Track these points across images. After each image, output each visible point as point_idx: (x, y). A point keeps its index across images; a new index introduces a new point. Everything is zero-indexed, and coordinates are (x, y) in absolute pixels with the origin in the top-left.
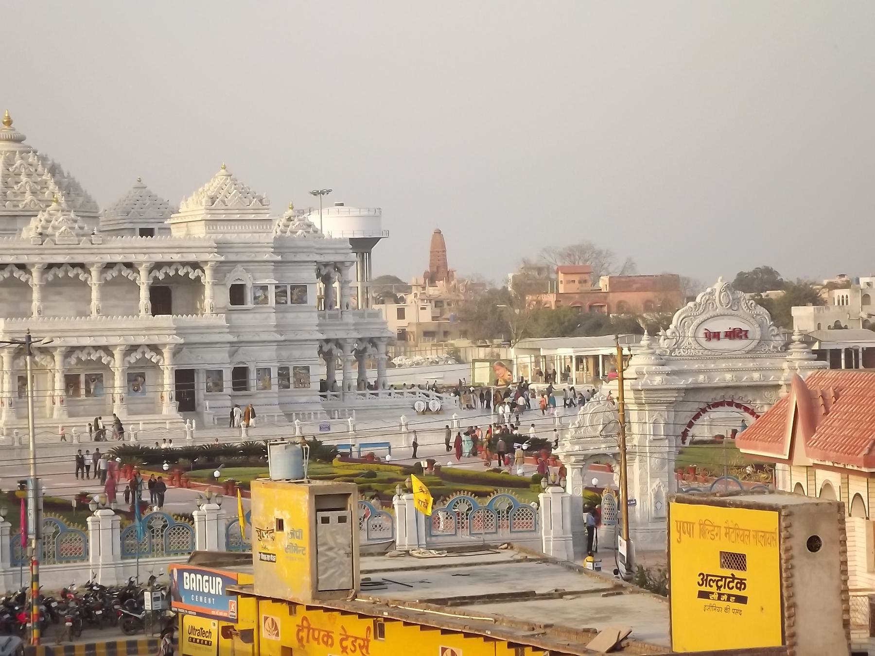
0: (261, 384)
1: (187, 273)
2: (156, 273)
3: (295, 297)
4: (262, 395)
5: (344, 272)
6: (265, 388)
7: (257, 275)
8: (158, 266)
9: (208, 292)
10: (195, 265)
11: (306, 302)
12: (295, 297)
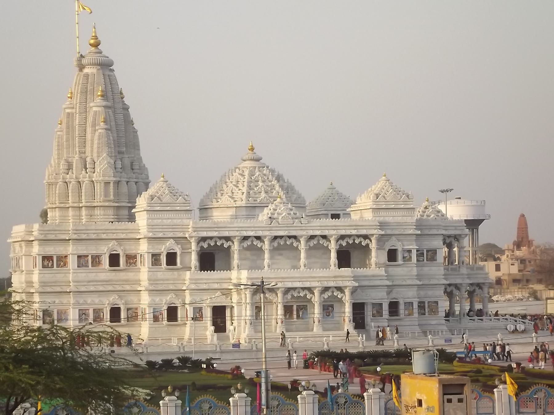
1: (361, 242)
2: (341, 242)
3: (429, 257)
4: (408, 319)
5: (461, 241)
6: (409, 315)
7: (405, 243)
8: (342, 237)
9: (373, 254)
10: (366, 237)
11: (436, 260)
12: (429, 257)
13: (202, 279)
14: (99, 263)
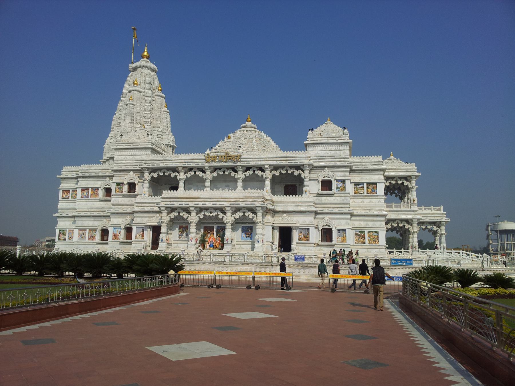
0: (340, 239)
6: (343, 241)
7: (338, 174)
9: (306, 182)
12: (370, 190)
13: (145, 203)
14: (97, 195)
